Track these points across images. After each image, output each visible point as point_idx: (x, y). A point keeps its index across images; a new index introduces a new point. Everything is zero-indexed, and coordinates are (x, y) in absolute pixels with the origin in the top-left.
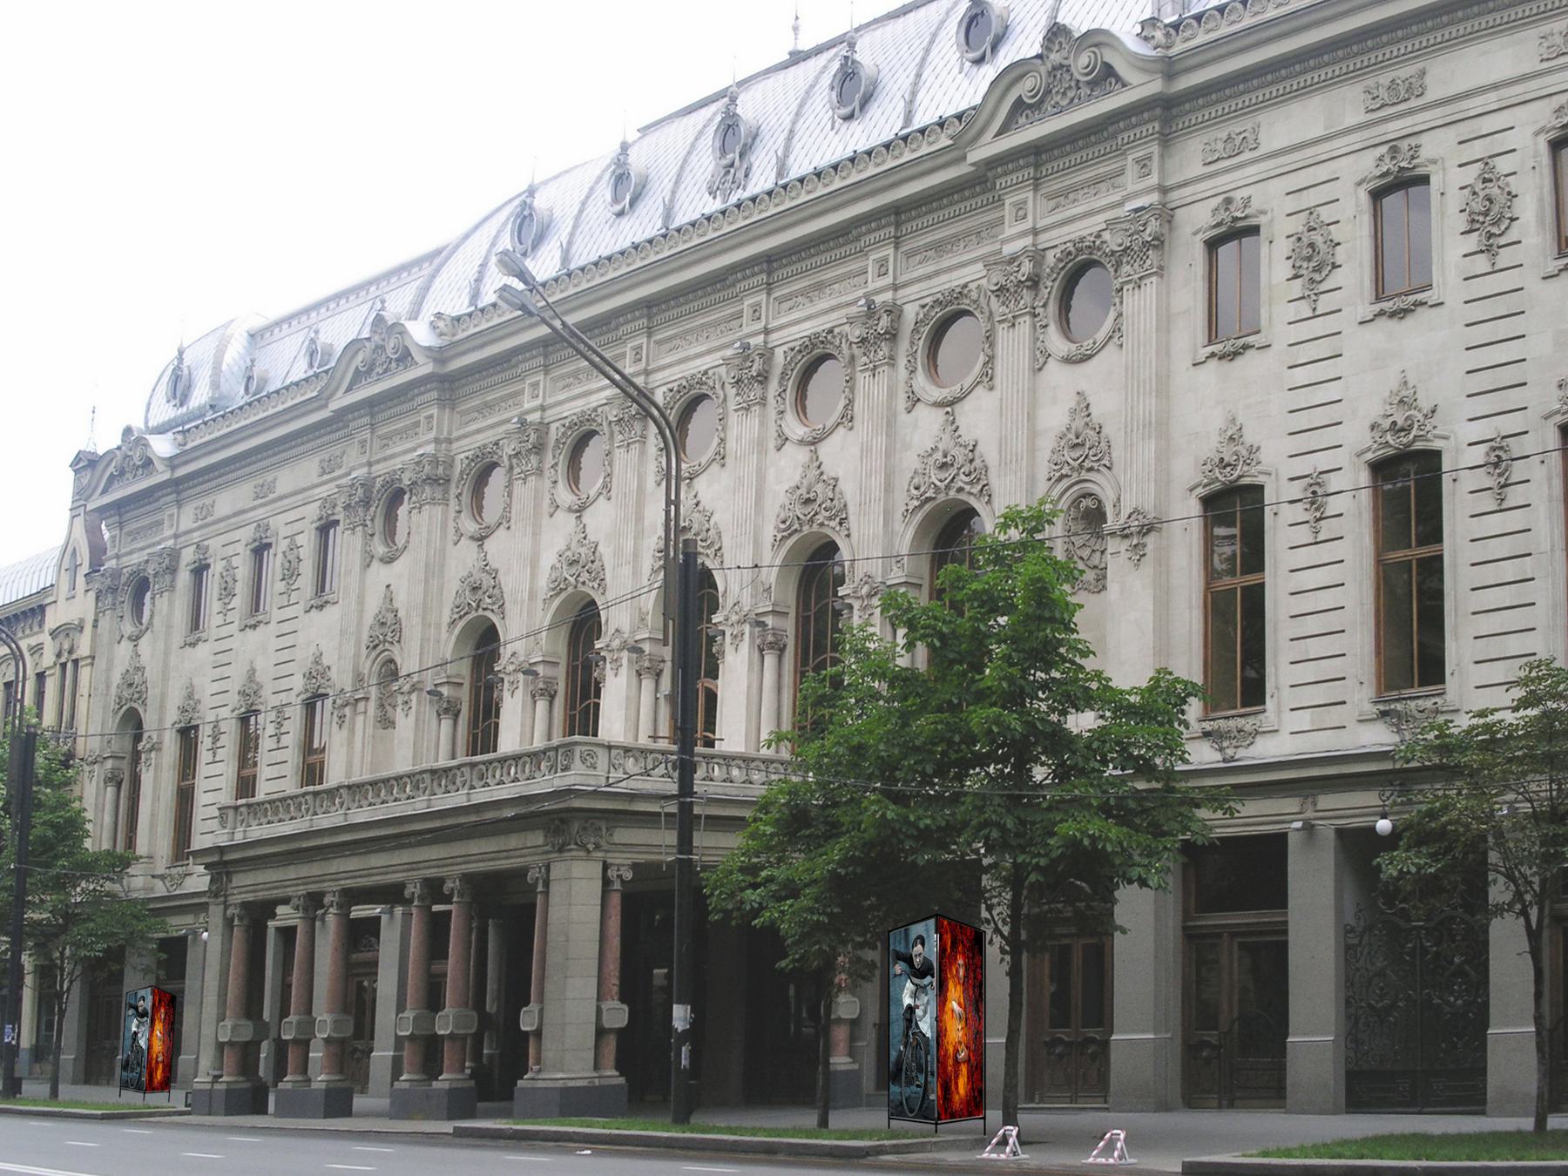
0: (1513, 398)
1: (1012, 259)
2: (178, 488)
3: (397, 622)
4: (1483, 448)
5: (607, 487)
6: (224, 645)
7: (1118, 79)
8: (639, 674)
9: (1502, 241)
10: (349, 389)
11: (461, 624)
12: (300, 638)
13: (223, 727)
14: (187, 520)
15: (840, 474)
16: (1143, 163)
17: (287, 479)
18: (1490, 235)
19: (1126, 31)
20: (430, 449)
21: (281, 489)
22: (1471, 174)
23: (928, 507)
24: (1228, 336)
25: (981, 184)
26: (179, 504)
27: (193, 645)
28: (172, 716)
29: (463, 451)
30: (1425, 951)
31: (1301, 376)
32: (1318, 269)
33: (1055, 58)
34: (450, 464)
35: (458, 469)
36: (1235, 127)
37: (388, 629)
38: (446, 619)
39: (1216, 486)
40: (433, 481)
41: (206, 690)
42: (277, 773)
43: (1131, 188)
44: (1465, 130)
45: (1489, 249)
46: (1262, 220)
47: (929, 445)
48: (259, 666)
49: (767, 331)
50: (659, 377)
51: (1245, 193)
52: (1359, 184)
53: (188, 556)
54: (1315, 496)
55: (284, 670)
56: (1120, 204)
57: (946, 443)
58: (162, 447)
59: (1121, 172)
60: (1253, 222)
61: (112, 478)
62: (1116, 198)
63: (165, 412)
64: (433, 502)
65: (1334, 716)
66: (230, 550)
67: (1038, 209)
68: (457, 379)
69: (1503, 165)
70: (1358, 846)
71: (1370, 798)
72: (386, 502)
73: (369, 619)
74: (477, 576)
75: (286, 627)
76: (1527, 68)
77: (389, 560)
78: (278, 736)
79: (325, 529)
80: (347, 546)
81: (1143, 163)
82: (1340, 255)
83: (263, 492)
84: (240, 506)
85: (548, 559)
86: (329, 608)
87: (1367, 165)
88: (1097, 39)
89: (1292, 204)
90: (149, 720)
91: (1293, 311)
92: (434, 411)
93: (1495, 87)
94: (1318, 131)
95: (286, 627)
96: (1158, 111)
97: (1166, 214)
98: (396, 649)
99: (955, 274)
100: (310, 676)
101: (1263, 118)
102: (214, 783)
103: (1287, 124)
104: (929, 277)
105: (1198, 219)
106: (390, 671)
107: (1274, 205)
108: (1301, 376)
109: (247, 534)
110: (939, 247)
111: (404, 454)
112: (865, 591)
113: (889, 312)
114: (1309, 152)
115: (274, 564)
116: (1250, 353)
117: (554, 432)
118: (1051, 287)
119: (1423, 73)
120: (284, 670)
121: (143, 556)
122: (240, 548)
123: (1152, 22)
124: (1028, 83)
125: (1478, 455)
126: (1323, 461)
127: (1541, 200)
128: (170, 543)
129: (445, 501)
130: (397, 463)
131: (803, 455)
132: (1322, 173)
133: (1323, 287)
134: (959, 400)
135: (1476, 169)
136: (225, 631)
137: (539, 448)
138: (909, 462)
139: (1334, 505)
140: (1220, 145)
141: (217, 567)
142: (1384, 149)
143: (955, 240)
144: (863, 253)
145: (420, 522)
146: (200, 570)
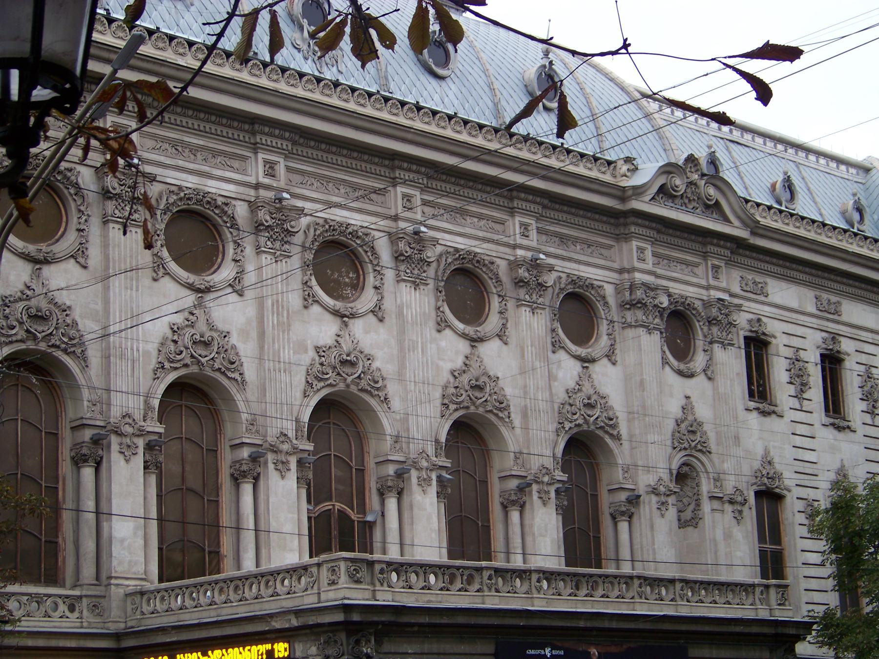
15: (499, 375)
23: (575, 430)
31: (799, 441)
39: (763, 488)
46: (773, 341)
52: (818, 347)
94: (794, 305)
99: (582, 268)
103: (784, 293)
108: (799, 441)
110: (563, 239)
112: (546, 479)
114: (794, 316)
116: (774, 416)
143: (576, 240)
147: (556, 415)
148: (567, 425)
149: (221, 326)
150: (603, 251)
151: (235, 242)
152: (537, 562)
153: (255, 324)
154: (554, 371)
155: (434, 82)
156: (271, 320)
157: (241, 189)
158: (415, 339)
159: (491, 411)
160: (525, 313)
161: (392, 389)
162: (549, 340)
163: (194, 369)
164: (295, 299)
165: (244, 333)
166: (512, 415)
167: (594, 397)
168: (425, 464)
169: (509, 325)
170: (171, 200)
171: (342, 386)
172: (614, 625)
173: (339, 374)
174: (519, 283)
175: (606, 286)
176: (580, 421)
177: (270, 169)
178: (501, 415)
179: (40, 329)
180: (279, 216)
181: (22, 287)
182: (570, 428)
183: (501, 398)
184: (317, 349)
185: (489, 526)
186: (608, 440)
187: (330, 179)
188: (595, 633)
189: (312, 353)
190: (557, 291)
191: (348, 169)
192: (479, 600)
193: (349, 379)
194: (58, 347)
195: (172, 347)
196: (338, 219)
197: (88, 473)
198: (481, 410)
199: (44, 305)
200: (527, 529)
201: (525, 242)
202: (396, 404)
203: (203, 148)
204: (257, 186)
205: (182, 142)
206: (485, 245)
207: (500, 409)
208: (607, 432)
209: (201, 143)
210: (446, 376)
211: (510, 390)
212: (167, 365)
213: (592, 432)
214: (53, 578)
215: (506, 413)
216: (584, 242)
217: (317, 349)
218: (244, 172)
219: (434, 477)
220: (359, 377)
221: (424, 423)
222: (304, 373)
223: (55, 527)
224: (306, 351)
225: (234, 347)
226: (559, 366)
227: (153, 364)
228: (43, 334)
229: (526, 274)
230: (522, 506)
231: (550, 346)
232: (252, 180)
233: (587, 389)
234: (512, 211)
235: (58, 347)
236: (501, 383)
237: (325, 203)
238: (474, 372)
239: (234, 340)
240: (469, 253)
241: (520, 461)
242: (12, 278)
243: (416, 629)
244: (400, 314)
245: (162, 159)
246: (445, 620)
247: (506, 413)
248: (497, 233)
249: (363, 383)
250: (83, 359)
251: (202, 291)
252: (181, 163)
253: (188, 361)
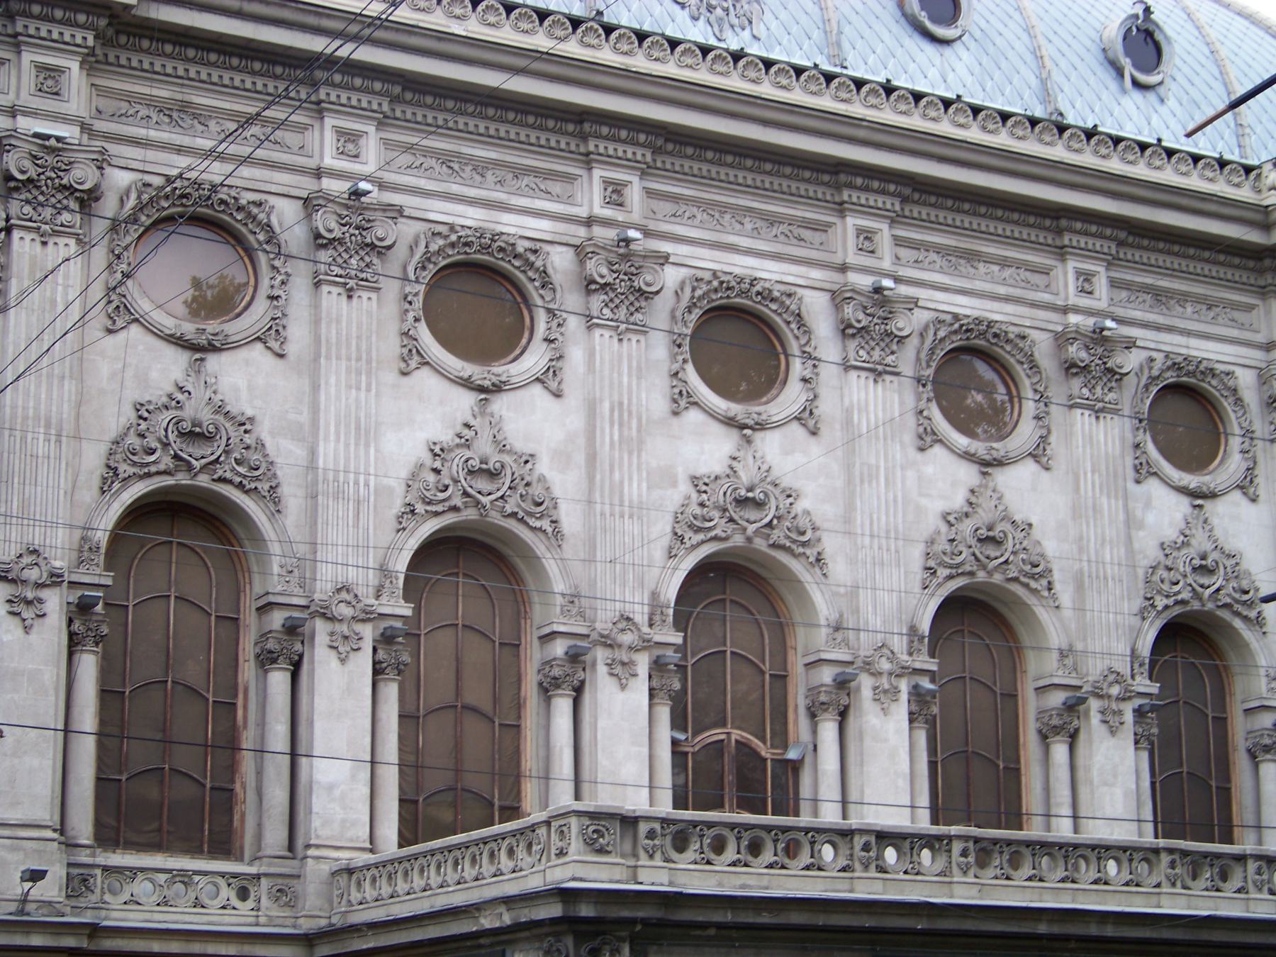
15: (1034, 520)
23: (1177, 610)
99: (1194, 342)
110: (1160, 297)
112: (1115, 690)
134: (1213, 495)
143: (1183, 298)
147: (1141, 585)
148: (1160, 602)
149: (520, 445)
150: (1236, 315)
151: (549, 311)
152: (1097, 832)
153: (581, 441)
154: (1139, 513)
155: (929, 49)
156: (607, 435)
157: (561, 227)
158: (873, 461)
159: (1015, 580)
160: (1082, 419)
161: (831, 545)
162: (1129, 462)
163: (470, 514)
164: (655, 399)
165: (562, 458)
166: (1058, 587)
167: (1214, 556)
168: (885, 665)
169: (1052, 439)
170: (434, 247)
171: (738, 540)
172: (1110, 931)
173: (731, 520)
174: (1071, 368)
175: (1239, 372)
176: (1185, 595)
177: (615, 195)
178: (1033, 584)
179: (198, 453)
180: (625, 267)
181: (170, 388)
182: (1166, 607)
183: (1035, 559)
184: (694, 480)
185: (1018, 770)
186: (1238, 623)
187: (724, 208)
188: (1073, 945)
189: (685, 488)
190: (1144, 381)
192: (846, 885)
193: (751, 528)
194: (230, 482)
195: (432, 478)
196: (737, 271)
197: (279, 680)
198: (997, 578)
199: (206, 416)
200: (1081, 774)
201: (1084, 302)
202: (839, 569)
203: (497, 164)
204: (589, 222)
205: (459, 155)
206: (1010, 308)
207: (1033, 577)
208: (1238, 614)
209: (493, 155)
210: (932, 522)
211: (1052, 546)
212: (420, 508)
213: (1210, 614)
214: (224, 845)
215: (1044, 582)
216: (1199, 300)
217: (694, 480)
218: (570, 200)
219: (904, 686)
220: (769, 525)
221: (888, 601)
222: (669, 518)
223: (232, 768)
224: (674, 484)
225: (542, 479)
226: (1148, 504)
227: (397, 506)
228: (203, 461)
229: (1083, 354)
230: (1073, 737)
231: (1131, 474)
232: (583, 212)
233: (1200, 542)
234: (1061, 253)
235: (230, 482)
236: (1036, 533)
237: (710, 245)
238: (984, 516)
239: (542, 466)
240: (978, 321)
241: (1069, 662)
242: (154, 375)
243: (712, 932)
244: (848, 422)
245: (423, 183)
246: (765, 918)
247: (1044, 582)
248: (1036, 288)
249: (777, 535)
250: (273, 499)
251: (488, 391)
252: (455, 188)
253: (458, 501)
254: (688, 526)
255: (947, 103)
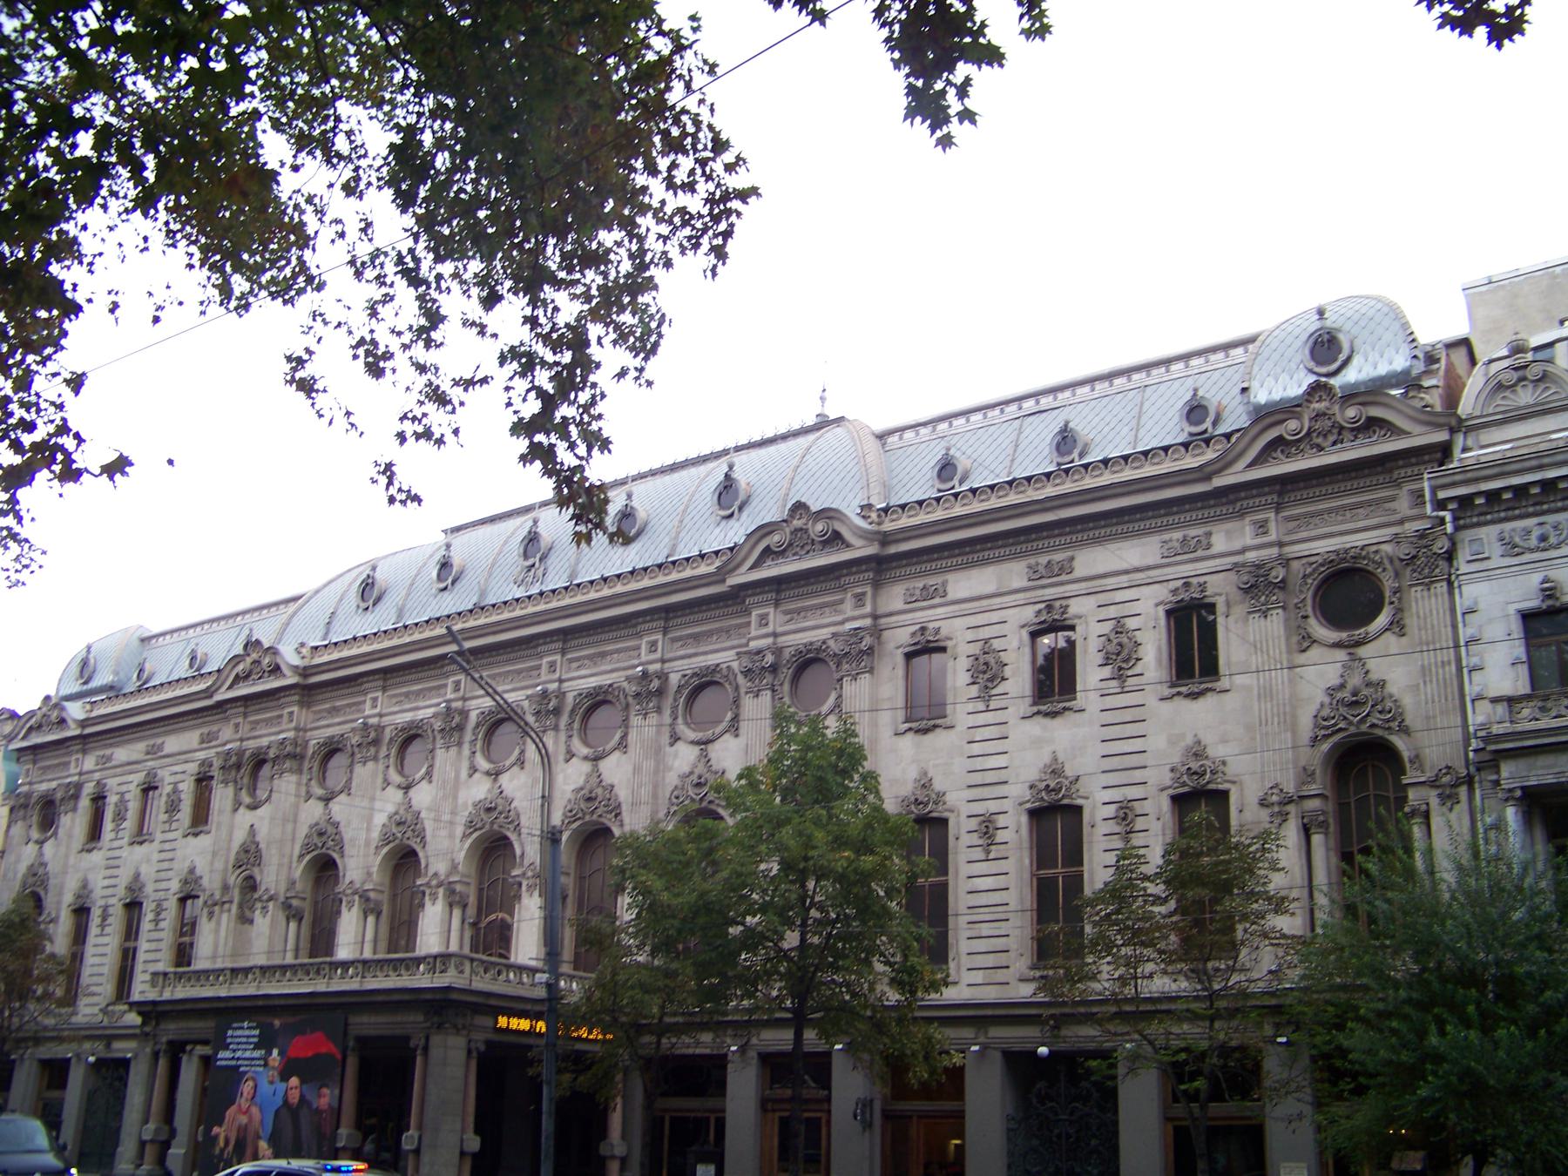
0: (1138, 776)
1: (759, 652)
2: (85, 741)
3: (258, 851)
4: (1113, 807)
5: (429, 775)
6: (116, 853)
7: (843, 541)
8: (451, 905)
9: (1130, 673)
10: (230, 688)
11: (308, 858)
12: (178, 853)
13: (111, 911)
14: (89, 763)
15: (616, 782)
16: (860, 598)
17: (172, 743)
18: (1120, 669)
19: (851, 511)
20: (291, 734)
21: (168, 749)
22: (1107, 627)
24: (924, 716)
25: (737, 598)
26: (85, 752)
27: (89, 851)
28: (68, 898)
29: (316, 737)
30: (1068, 1136)
31: (976, 749)
32: (991, 680)
33: (797, 523)
34: (306, 747)
35: (310, 751)
36: (931, 581)
37: (250, 855)
38: (297, 852)
40: (292, 756)
41: (98, 883)
42: (154, 952)
43: (850, 614)
44: (1103, 598)
45: (1120, 676)
46: (949, 644)
47: (687, 769)
48: (144, 870)
49: (561, 681)
50: (474, 703)
51: (936, 625)
53: (89, 789)
54: (987, 828)
55: (163, 875)
56: (842, 623)
57: (701, 769)
58: (76, 711)
59: (842, 601)
60: (942, 644)
61: (31, 728)
62: (839, 618)
63: (74, 687)
64: (291, 771)
65: (1000, 976)
66: (124, 788)
67: (776, 620)
68: (318, 686)
69: (1131, 623)
70: (1019, 1064)
71: (1032, 1032)
72: (251, 768)
73: (236, 846)
74: (323, 825)
75: (167, 846)
76: (1151, 561)
77: (253, 807)
78: (156, 921)
79: (203, 781)
80: (222, 796)
81: (860, 598)
82: (1007, 671)
83: (153, 752)
84: (134, 757)
85: (380, 819)
86: (202, 837)
87: (1028, 614)
88: (827, 514)
89: (970, 635)
90: (49, 902)
91: (971, 707)
92: (295, 709)
93: (1127, 572)
95: (167, 846)
96: (873, 565)
97: (877, 632)
98: (256, 870)
100: (185, 882)
101: (951, 577)
102: (101, 950)
103: (966, 583)
104: (690, 656)
105: (900, 637)
106: (250, 885)
107: (960, 633)
108: (976, 749)
109: (138, 778)
110: (696, 637)
111: (268, 735)
113: (659, 678)
114: (985, 603)
115: (159, 802)
116: (938, 731)
117: (388, 734)
118: (786, 673)
119: (1072, 559)
120: (163, 875)
121: (54, 784)
122: (132, 787)
123: (870, 506)
124: (776, 538)
125: (1110, 811)
126: (993, 806)
127: (1159, 649)
128: (76, 778)
129: (300, 771)
130: (265, 742)
131: (586, 767)
132: (995, 617)
133: (994, 692)
135: (1109, 626)
136: (116, 844)
137: (376, 742)
138: (672, 779)
139: (1001, 836)
140: (918, 592)
141: (112, 799)
142: (1042, 606)
143: (709, 634)
144: (639, 635)
145: (286, 786)
146: (99, 799)
165: (429, 809)
189: (470, 808)
191: (508, 662)
210: (569, 795)
211: (623, 794)
216: (719, 631)
254: (471, 825)
255: (632, 573)
